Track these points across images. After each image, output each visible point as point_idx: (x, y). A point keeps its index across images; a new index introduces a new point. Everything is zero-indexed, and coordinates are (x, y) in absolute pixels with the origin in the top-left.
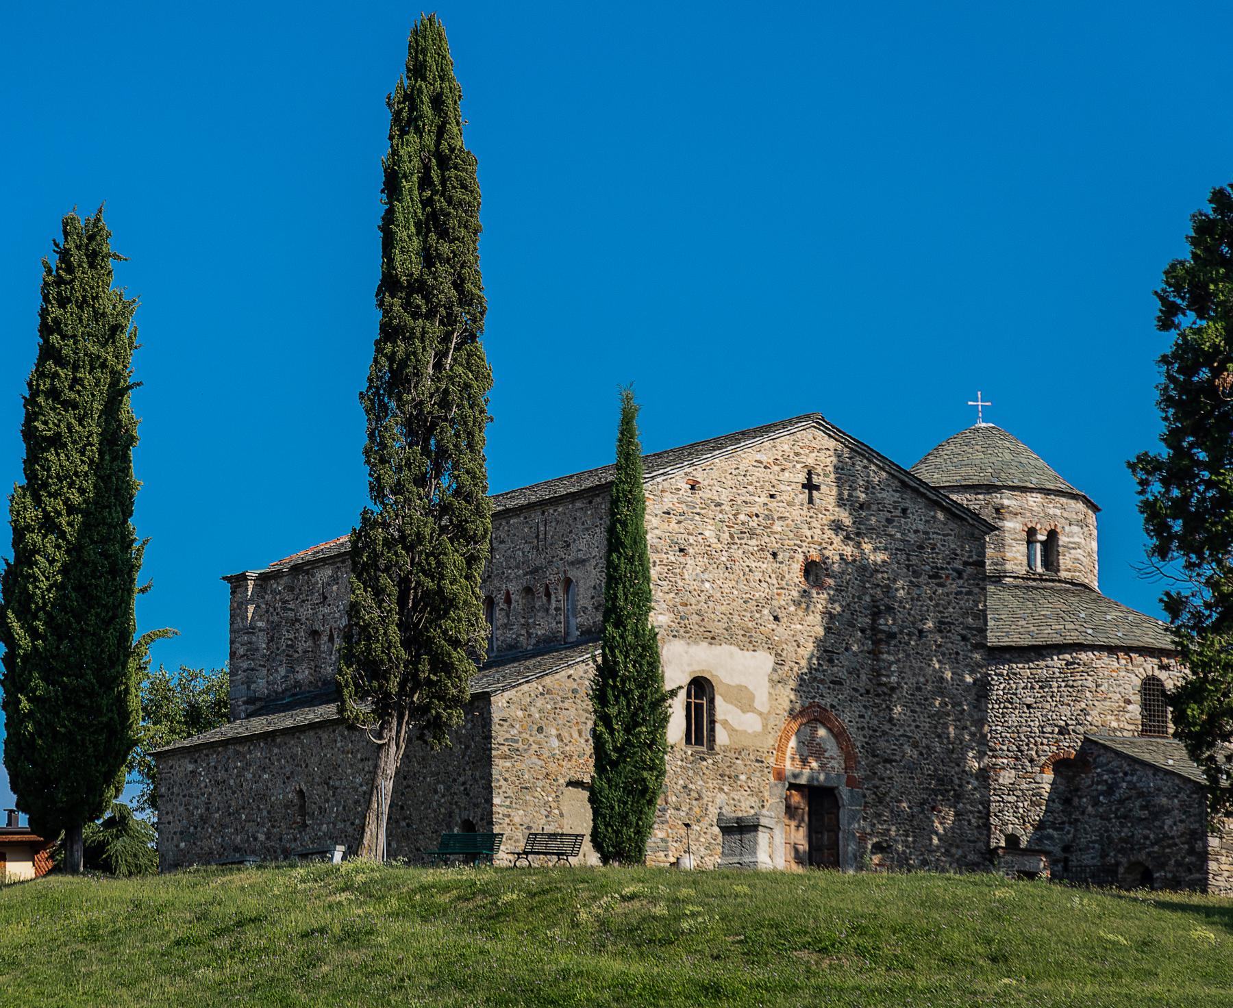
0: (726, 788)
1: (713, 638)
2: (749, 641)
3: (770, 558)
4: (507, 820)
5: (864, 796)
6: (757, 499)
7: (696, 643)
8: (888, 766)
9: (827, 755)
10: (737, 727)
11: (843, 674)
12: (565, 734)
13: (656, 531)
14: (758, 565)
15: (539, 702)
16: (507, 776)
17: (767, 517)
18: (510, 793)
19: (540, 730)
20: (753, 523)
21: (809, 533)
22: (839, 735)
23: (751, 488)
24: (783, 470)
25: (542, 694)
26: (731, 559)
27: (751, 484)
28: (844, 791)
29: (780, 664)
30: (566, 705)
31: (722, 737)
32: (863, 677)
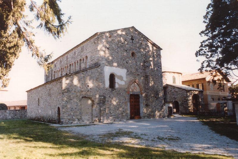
11: (139, 73)
26: (118, 51)
29: (128, 71)
31: (117, 86)
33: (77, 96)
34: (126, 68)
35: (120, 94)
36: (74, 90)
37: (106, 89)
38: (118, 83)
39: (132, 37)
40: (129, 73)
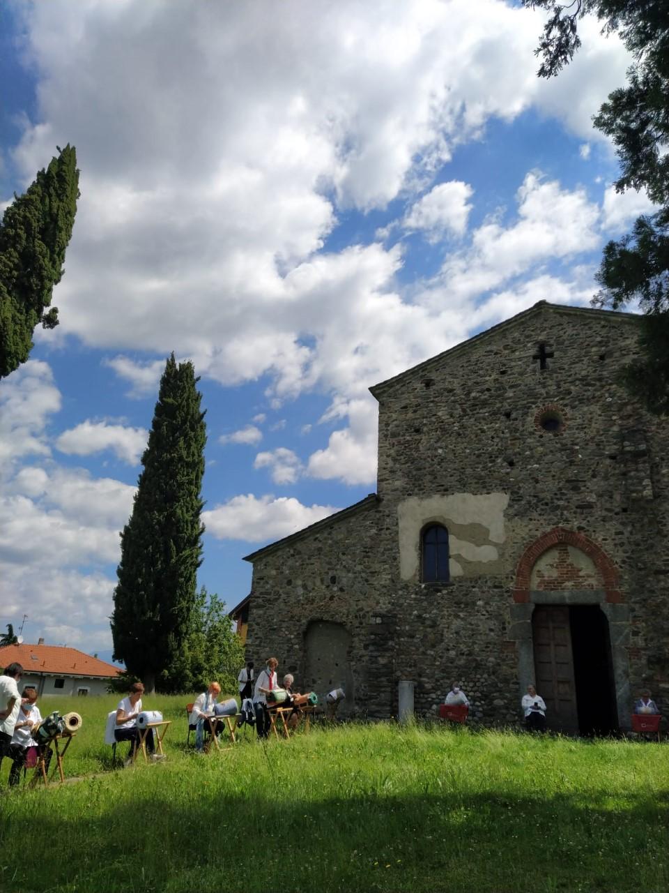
0: (462, 615)
1: (446, 490)
2: (483, 485)
3: (503, 418)
4: (255, 657)
5: (633, 610)
6: (487, 378)
7: (429, 496)
8: (662, 577)
9: (581, 574)
10: (471, 560)
11: (592, 498)
12: (309, 584)
13: (395, 422)
14: (489, 426)
15: (290, 562)
16: (259, 621)
17: (498, 389)
18: (260, 635)
19: (289, 583)
20: (486, 396)
21: (543, 391)
22: (593, 552)
23: (481, 372)
24: (513, 352)
25: (293, 555)
26: (463, 427)
27: (482, 369)
28: (606, 608)
29: (516, 498)
30: (312, 561)
31: (455, 569)
32: (617, 497)
33: (292, 617)
34: (505, 486)
35: (474, 603)
36: (283, 596)
37: (406, 587)
38: (464, 554)
39: (542, 346)
40: (519, 508)
